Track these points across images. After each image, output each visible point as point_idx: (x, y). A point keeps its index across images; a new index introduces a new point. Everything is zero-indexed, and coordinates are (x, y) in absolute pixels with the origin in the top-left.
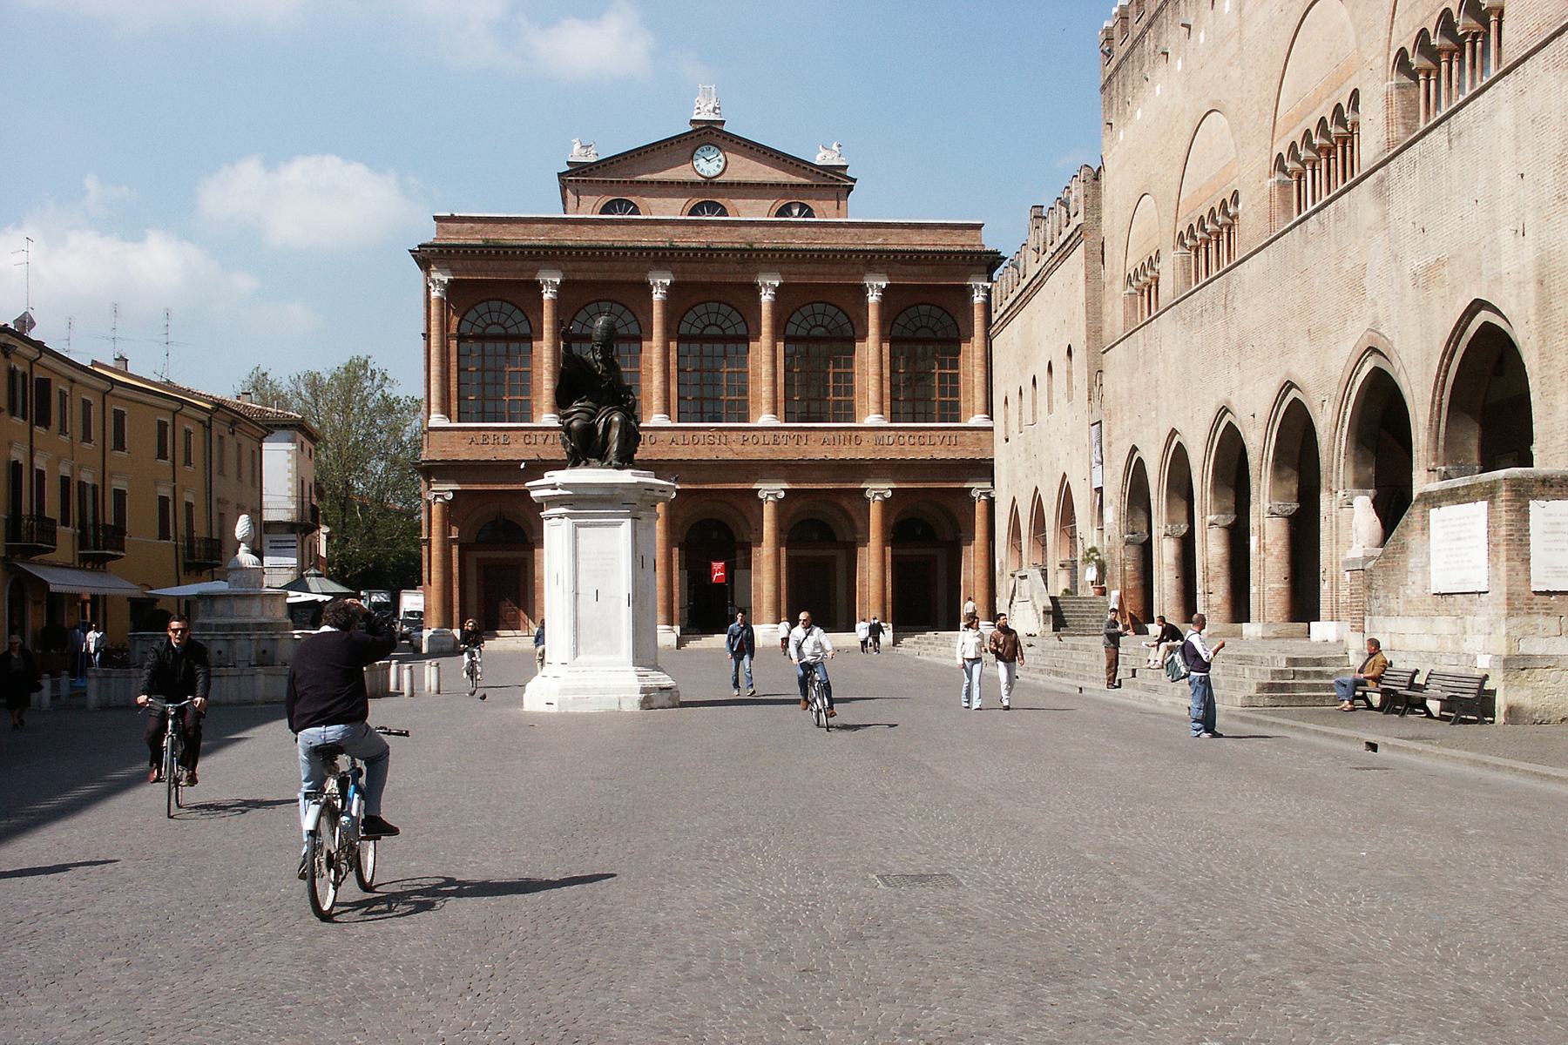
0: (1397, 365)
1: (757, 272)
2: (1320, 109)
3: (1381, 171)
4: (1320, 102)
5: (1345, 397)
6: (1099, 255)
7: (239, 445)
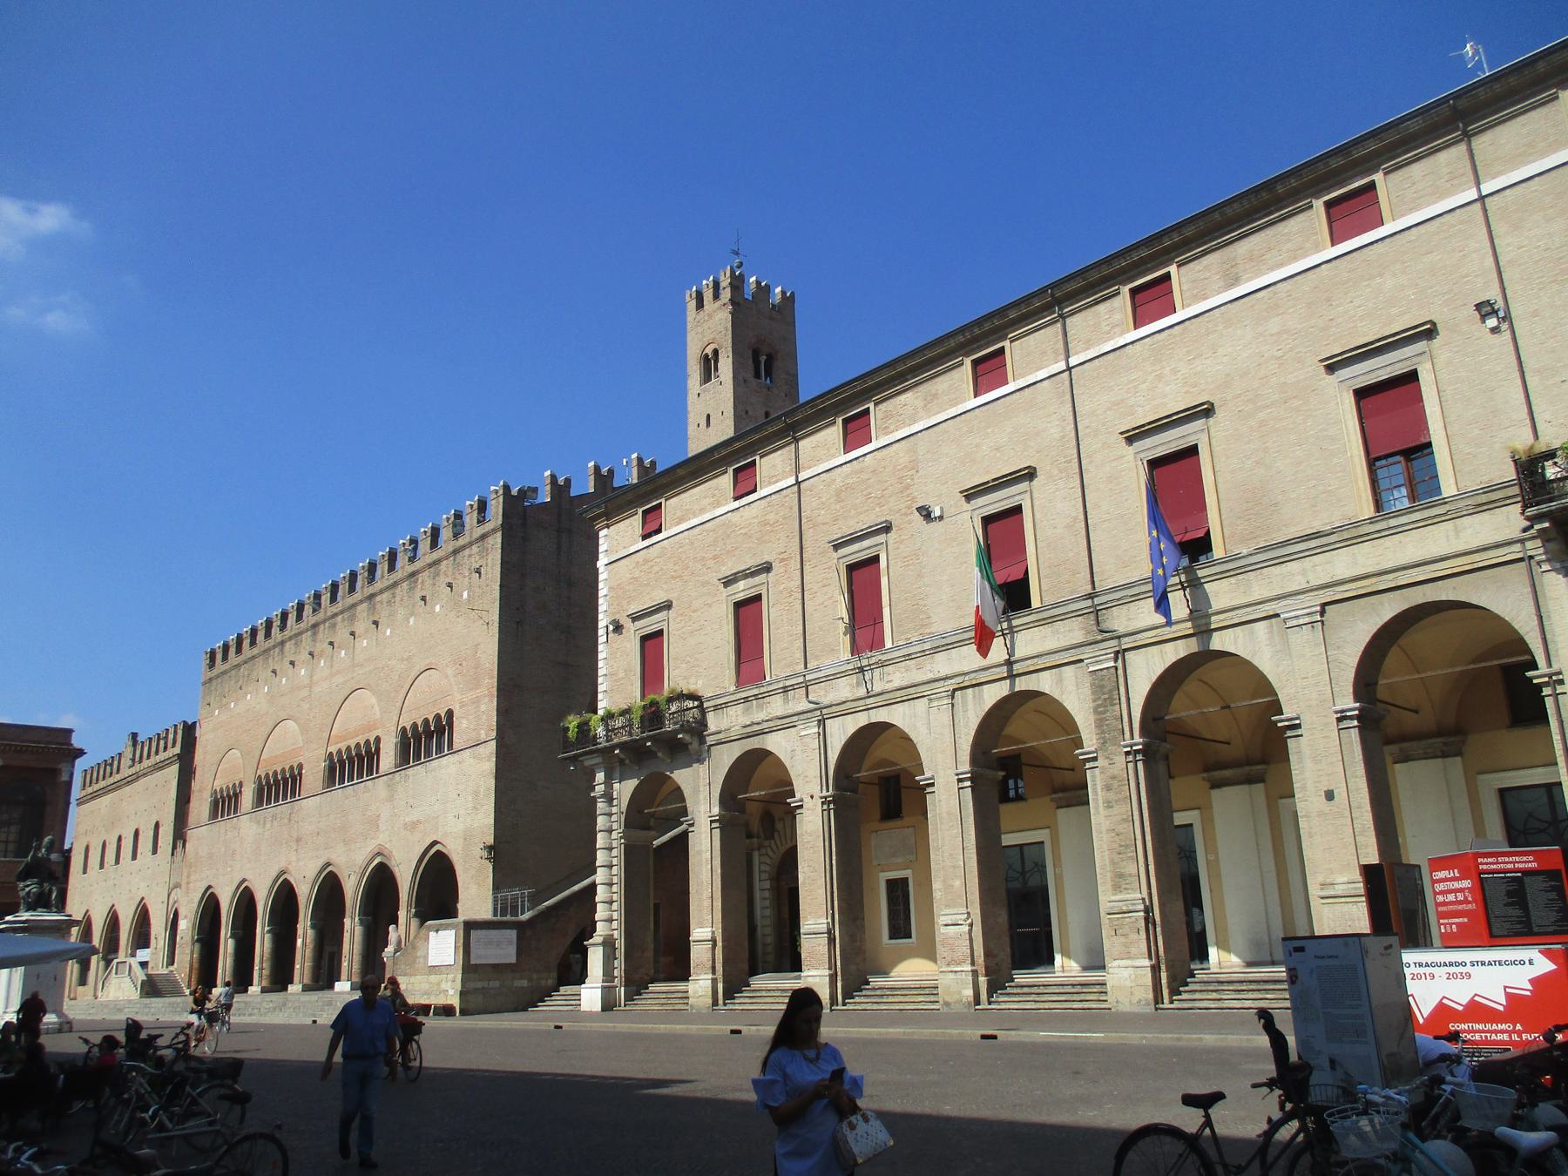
0: (393, 863)
2: (351, 741)
4: (357, 736)
5: (363, 874)
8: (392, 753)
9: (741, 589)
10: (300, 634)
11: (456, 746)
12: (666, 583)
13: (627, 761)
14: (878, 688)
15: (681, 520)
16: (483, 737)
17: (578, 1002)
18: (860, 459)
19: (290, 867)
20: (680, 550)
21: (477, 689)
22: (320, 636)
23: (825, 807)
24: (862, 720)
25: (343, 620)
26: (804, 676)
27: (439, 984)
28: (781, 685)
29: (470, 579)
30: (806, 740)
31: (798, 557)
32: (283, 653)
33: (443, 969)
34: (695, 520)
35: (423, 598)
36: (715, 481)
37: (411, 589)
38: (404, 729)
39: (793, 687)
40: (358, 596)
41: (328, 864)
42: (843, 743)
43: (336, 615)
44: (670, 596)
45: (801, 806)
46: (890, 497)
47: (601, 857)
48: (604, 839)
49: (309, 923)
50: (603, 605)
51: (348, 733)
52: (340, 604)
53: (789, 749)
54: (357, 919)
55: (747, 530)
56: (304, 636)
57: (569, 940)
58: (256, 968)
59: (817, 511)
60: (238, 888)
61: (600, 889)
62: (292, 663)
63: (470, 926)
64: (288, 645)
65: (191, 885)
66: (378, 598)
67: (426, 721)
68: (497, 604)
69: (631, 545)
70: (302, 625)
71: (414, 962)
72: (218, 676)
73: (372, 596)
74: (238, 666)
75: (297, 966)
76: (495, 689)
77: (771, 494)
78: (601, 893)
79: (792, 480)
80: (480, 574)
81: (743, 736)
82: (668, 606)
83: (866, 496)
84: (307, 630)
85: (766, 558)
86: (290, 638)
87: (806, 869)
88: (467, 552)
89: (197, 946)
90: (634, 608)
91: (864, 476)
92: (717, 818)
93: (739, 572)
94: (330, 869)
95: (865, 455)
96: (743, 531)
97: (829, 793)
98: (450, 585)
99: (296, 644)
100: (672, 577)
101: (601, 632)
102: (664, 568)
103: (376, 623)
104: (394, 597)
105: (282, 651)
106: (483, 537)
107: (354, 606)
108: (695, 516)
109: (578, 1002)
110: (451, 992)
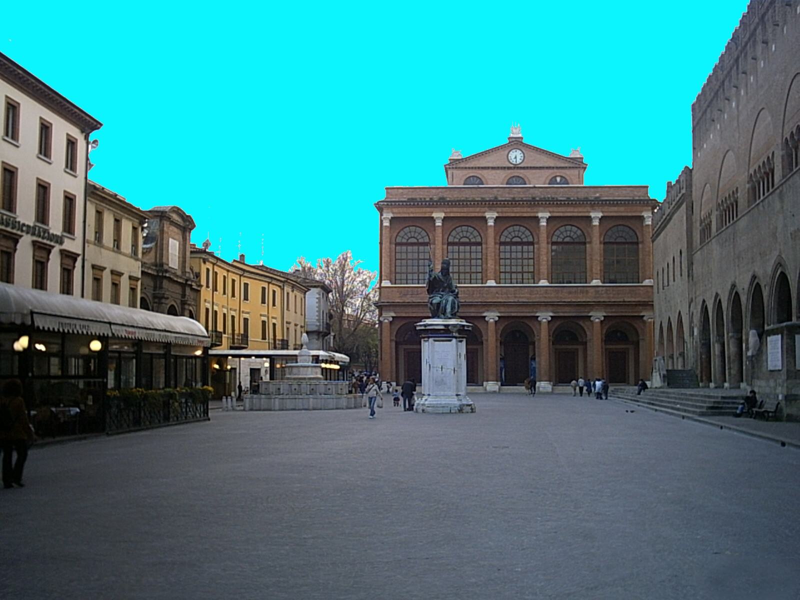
6: (690, 209)
7: (296, 296)
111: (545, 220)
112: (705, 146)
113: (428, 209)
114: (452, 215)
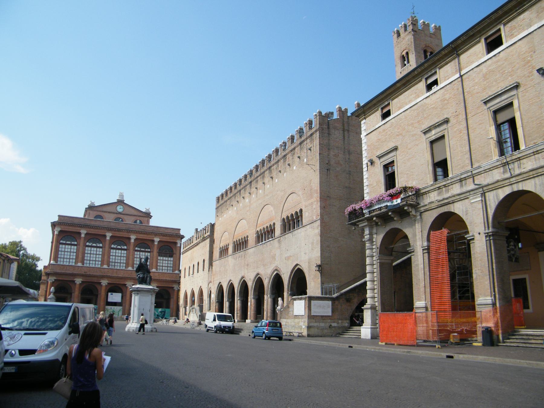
0: (281, 273)
1: (130, 235)
3: (279, 238)
5: (270, 278)
8: (279, 229)
9: (433, 134)
10: (246, 186)
11: (304, 224)
12: (394, 138)
13: (379, 224)
14: (517, 172)
15: (400, 108)
16: (315, 218)
17: (359, 334)
18: (497, 55)
19: (245, 275)
20: (401, 122)
21: (312, 199)
22: (253, 186)
23: (488, 239)
24: (507, 191)
25: (260, 178)
26: (472, 171)
27: (299, 323)
28: (458, 178)
29: (307, 153)
30: (474, 204)
31: (464, 112)
32: (240, 194)
33: (300, 317)
34: (407, 106)
35: (289, 165)
36: (416, 86)
37: (285, 162)
38: (284, 219)
39: (465, 179)
40: (265, 168)
41: (258, 274)
42: (497, 203)
43: (258, 177)
44: (397, 144)
45: (473, 239)
46: (517, 70)
47: (368, 268)
48: (370, 260)
49: (252, 297)
50: (365, 154)
51: (263, 223)
52: (259, 173)
53: (464, 210)
54: (269, 295)
55: (434, 105)
56: (247, 187)
57: (354, 306)
58: (235, 313)
59: (473, 87)
60: (229, 283)
61: (368, 283)
62: (243, 198)
63: (311, 299)
64: (242, 191)
65: (214, 282)
66: (272, 168)
67: (292, 215)
68: (318, 161)
69: (377, 124)
70: (246, 183)
71: (288, 313)
72: (220, 206)
73: (270, 168)
74: (226, 201)
75: (249, 313)
76: (319, 198)
77: (446, 85)
78: (369, 286)
79: (458, 75)
80: (311, 150)
81: (439, 206)
82: (395, 149)
83: (502, 73)
84: (248, 185)
85: (445, 116)
86: (243, 188)
87: (477, 271)
88: (305, 143)
89: (217, 304)
90: (379, 153)
91: (499, 64)
92: (426, 248)
93: (431, 126)
94: (259, 276)
95: (499, 52)
96: (432, 106)
97: (490, 231)
98: (299, 157)
99: (244, 190)
100: (397, 135)
101: (364, 166)
102: (393, 132)
103: (272, 178)
104: (278, 166)
105: (240, 193)
106: (312, 135)
107: (264, 172)
108: (406, 104)
109: (359, 334)
110: (303, 327)
111: (134, 239)
112: (225, 216)
113: (79, 228)
114: (90, 232)
